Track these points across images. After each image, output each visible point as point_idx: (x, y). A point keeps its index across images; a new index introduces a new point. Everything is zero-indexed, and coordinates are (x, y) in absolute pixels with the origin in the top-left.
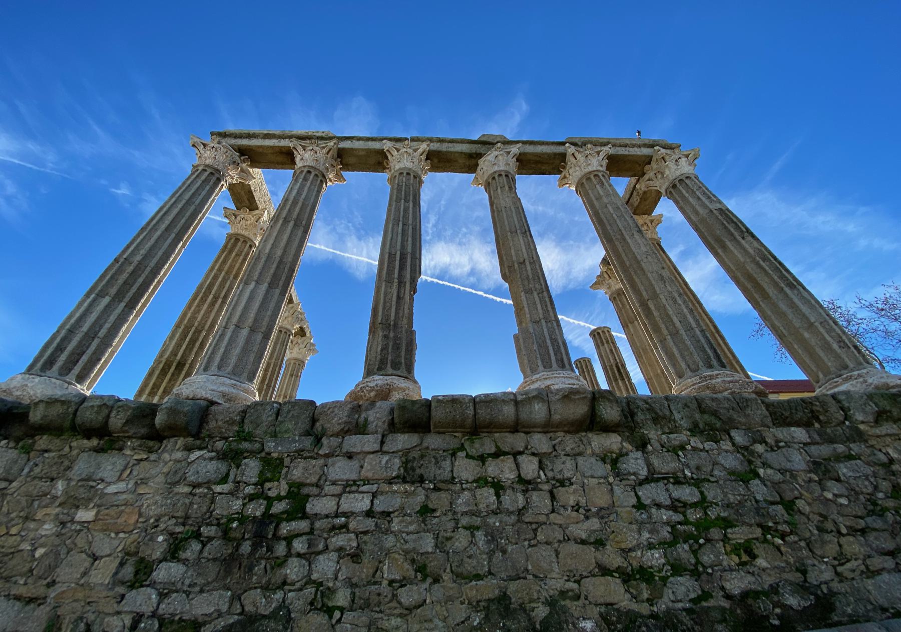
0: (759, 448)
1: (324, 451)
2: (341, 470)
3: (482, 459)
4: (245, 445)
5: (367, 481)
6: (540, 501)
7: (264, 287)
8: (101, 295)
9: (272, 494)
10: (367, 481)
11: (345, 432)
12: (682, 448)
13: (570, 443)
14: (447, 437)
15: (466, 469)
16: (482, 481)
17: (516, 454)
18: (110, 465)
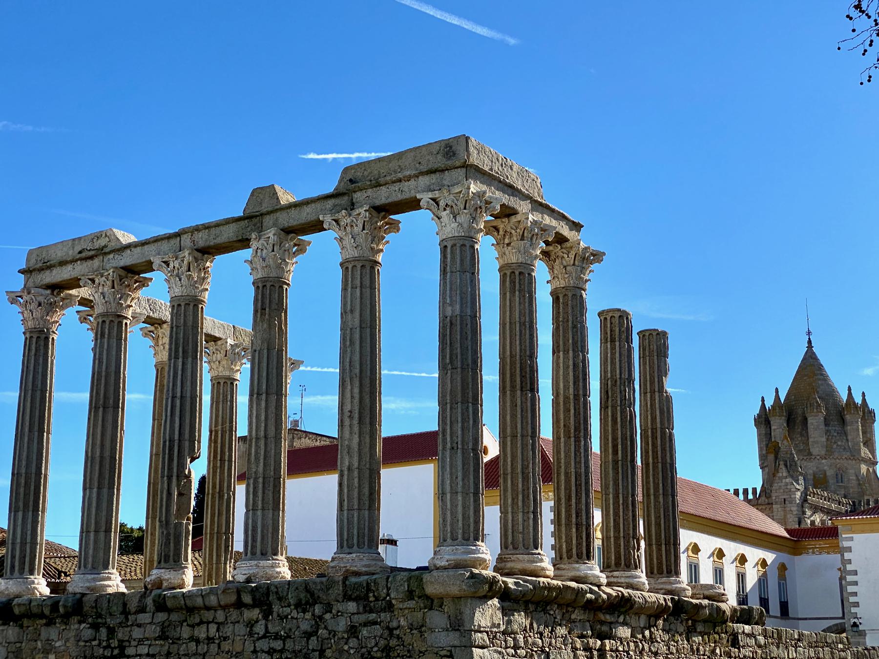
0: (328, 616)
1: (130, 623)
2: (137, 633)
3: (192, 626)
4: (100, 620)
5: (148, 639)
6: (214, 648)
7: (95, 490)
8: (16, 511)
9: (113, 645)
10: (148, 639)
11: (138, 612)
12: (286, 617)
13: (234, 614)
14: (180, 614)
15: (186, 632)
16: (192, 639)
17: (208, 623)
18: (53, 633)
